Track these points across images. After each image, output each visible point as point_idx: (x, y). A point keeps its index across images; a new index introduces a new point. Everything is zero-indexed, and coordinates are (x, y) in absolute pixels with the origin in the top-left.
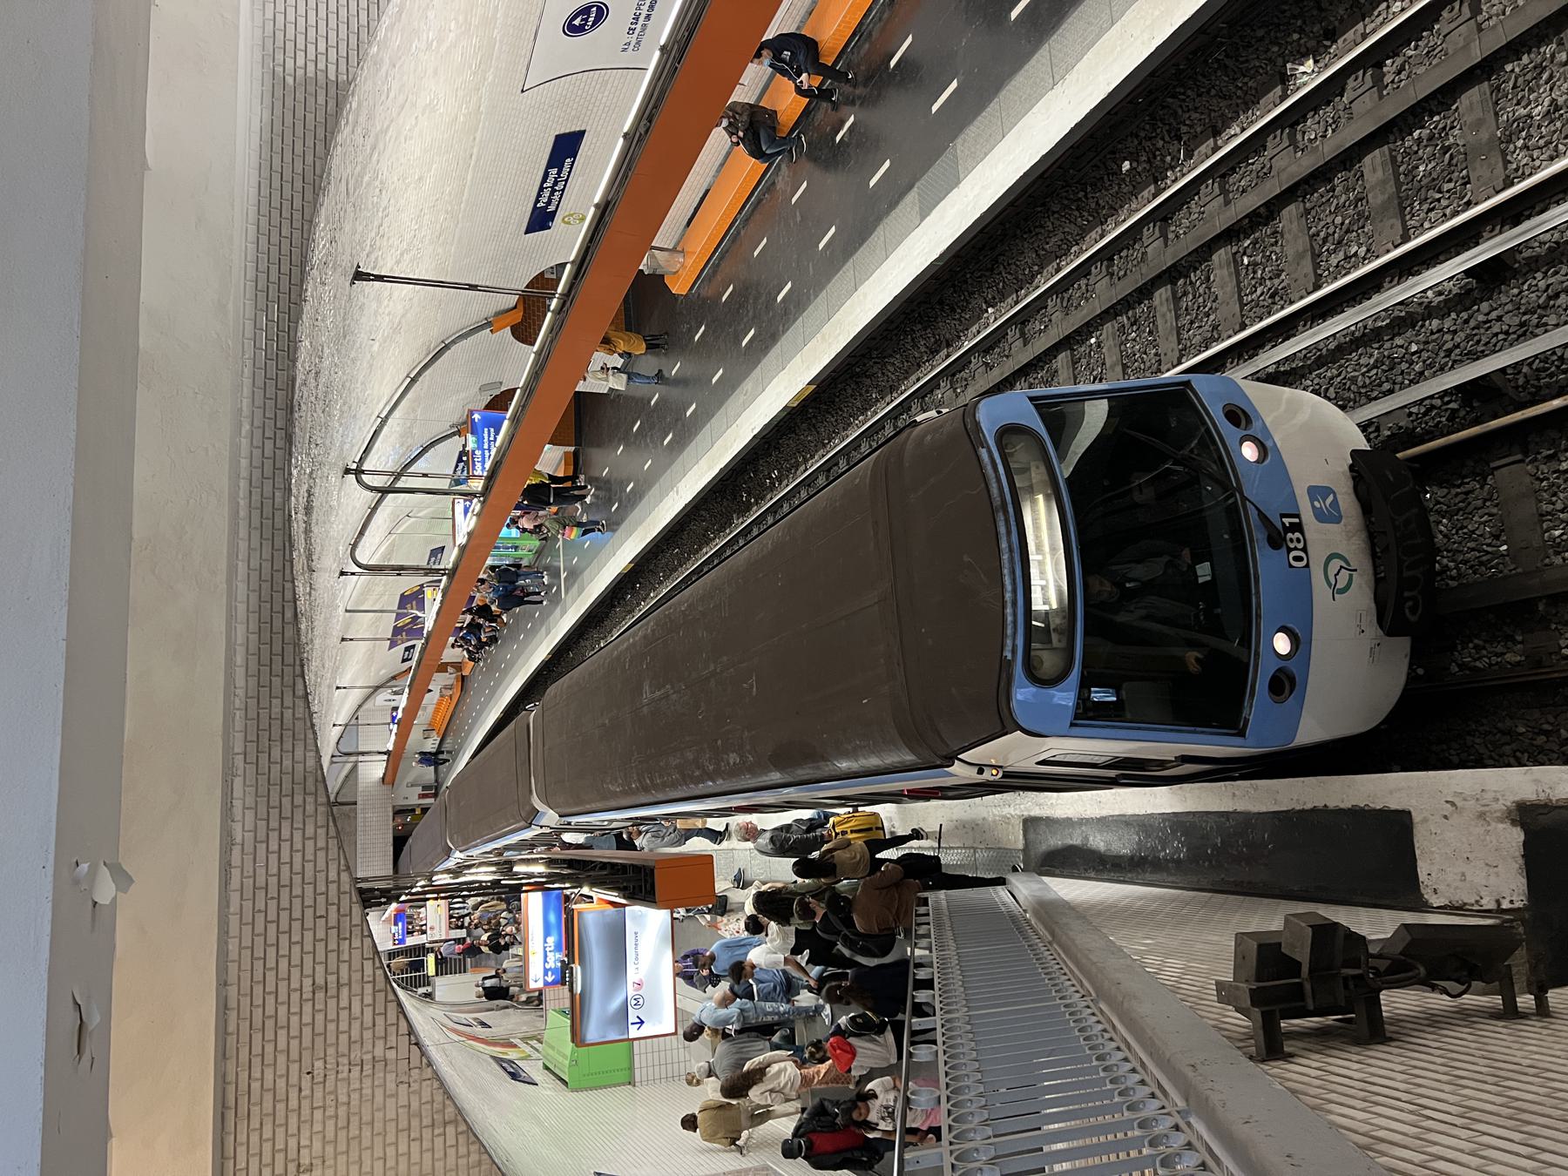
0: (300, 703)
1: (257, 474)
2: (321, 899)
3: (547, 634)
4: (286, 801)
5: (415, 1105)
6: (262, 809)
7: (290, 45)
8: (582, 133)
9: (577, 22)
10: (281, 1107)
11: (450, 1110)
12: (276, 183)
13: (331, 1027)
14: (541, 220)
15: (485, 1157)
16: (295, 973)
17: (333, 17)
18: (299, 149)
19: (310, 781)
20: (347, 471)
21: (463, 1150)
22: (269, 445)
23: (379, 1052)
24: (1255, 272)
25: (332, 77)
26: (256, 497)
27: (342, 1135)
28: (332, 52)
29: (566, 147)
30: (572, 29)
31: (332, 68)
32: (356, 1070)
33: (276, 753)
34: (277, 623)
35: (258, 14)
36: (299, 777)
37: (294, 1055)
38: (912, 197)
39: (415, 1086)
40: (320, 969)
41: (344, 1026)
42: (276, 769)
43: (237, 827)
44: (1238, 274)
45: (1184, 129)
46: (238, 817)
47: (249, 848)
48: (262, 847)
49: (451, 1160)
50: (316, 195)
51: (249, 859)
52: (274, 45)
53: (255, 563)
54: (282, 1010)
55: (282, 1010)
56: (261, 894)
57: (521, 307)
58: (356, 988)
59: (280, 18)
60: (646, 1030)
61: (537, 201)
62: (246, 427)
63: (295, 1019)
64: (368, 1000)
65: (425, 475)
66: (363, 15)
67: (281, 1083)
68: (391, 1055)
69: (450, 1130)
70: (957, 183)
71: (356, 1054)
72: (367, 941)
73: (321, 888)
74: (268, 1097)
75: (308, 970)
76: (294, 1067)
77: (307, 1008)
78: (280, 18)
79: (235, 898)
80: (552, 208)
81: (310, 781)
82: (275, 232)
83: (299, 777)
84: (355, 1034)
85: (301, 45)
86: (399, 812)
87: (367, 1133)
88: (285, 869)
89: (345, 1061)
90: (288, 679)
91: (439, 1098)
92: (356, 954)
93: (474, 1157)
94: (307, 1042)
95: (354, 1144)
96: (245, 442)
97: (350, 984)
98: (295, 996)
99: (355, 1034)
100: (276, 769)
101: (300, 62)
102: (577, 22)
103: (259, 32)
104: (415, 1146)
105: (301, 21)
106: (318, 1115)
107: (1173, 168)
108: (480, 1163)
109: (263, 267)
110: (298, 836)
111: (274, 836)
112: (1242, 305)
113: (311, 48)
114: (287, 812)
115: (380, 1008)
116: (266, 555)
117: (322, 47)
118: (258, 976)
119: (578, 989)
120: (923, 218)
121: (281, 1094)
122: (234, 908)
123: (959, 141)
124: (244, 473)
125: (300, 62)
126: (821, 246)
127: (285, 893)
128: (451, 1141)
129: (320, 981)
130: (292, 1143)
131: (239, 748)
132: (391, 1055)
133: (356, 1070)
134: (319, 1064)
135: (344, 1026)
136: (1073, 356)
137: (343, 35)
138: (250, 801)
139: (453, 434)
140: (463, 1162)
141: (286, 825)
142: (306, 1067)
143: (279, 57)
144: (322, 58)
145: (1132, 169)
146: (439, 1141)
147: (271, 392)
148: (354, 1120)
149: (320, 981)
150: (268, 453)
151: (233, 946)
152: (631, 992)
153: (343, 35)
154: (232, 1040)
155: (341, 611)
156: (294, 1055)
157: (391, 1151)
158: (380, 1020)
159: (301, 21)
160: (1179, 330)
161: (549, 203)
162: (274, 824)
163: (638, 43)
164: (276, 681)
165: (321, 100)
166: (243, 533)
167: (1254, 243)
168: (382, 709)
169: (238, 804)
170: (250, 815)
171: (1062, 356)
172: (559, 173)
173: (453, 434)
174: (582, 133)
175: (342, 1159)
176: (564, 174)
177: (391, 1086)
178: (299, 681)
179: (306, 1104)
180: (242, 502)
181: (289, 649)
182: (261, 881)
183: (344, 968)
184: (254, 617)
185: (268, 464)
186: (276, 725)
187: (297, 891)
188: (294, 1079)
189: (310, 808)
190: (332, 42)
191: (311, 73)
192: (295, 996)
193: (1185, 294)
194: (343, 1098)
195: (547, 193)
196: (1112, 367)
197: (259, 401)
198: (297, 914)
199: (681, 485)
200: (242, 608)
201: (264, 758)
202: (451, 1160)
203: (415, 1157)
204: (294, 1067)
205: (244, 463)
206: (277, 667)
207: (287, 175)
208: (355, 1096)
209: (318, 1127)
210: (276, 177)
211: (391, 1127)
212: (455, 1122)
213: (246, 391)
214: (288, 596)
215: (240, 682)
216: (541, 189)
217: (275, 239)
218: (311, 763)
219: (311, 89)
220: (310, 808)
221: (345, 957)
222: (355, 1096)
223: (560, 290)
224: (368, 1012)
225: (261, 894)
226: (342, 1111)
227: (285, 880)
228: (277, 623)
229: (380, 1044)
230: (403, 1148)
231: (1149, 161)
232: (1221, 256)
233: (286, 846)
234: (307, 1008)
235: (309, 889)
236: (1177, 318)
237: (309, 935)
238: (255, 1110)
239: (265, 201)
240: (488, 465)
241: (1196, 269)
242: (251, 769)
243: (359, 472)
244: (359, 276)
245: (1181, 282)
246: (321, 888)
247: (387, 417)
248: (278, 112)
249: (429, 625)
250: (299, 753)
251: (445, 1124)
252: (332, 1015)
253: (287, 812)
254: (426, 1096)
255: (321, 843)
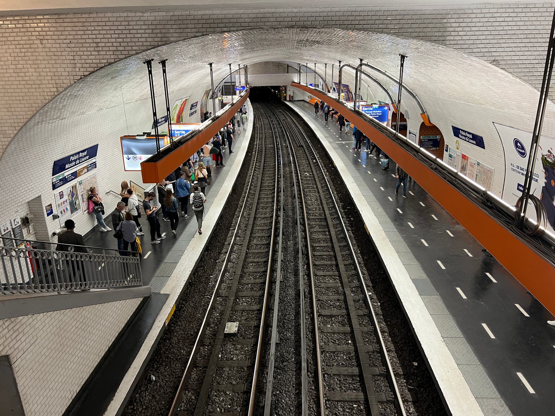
0: (192, 35)
1: (278, 15)
2: (126, 44)
3: (325, 137)
4: (158, 31)
5: (62, 78)
6: (155, 23)
7: (461, 20)
8: (484, 148)
9: (518, 144)
10: (59, 33)
11: (61, 90)
12: (398, 17)
13: (85, 49)
14: (457, 132)
15: (47, 101)
16: (102, 36)
17: (476, 37)
18: (413, 26)
19: (166, 39)
20: (361, 60)
21: (49, 94)
22: (290, 19)
23: (78, 65)
24: (349, 409)
25: (448, 38)
26: (268, 15)
27: (52, 54)
28: (460, 38)
29: (479, 141)
30: (516, 142)
31: (452, 38)
32: (71, 58)
33: (175, 26)
34: (222, 25)
35: (475, 7)
36: (167, 35)
37: (76, 37)
38: (424, 276)
39: (68, 77)
40: (103, 45)
41: (86, 53)
42: (169, 27)
43: (149, 14)
44: (351, 402)
45: (422, 390)
46: (152, 14)
47: (142, 18)
48: (142, 23)
49: (46, 90)
50: (394, 34)
51: (138, 19)
52: (461, 14)
53: (243, 16)
54: (90, 32)
55: (90, 32)
56: (126, 23)
57: (430, 125)
58: (98, 57)
59: (474, 16)
60: (126, 160)
61: (462, 130)
62: (295, 10)
63: (87, 36)
64: (94, 61)
65: (360, 89)
66: (478, 50)
67: (67, 33)
68: (77, 69)
69: (55, 89)
70: (420, 295)
71: (77, 57)
72: (113, 61)
73: (130, 44)
74: (62, 29)
75: (103, 40)
76: (72, 37)
77: (91, 41)
78: (474, 16)
79: (125, 14)
80: (460, 136)
81: (166, 39)
82: (377, 18)
83: (167, 35)
84: (83, 57)
85: (461, 25)
86: (285, 87)
87: (53, 62)
88: (135, 31)
89: (75, 54)
90: (201, 30)
91: (65, 86)
92: (108, 57)
93: (47, 98)
94: (80, 41)
95: (49, 58)
96: (289, 10)
97: (99, 55)
98: (94, 36)
99: (83, 57)
100: (169, 27)
101: (453, 25)
102: (518, 144)
103: (467, 7)
104: (49, 78)
105: (473, 24)
106: (58, 45)
107: (407, 383)
108: (45, 99)
109: (361, 14)
110: (147, 35)
111: (146, 27)
112: (338, 401)
113: (461, 29)
114: (155, 31)
115: (92, 65)
116: (247, 20)
117: (461, 33)
118: (100, 24)
119: (137, 138)
120: (412, 280)
121: (64, 33)
122: (122, 14)
123: (439, 297)
124: (277, 10)
125: (453, 25)
126: (423, 241)
127: (127, 32)
128: (52, 90)
129: (100, 45)
130: (49, 37)
131: (176, 13)
132: (77, 69)
133: (71, 58)
134: (73, 45)
135: (86, 53)
136: (347, 333)
137: (467, 42)
138: (158, 18)
139: (392, 101)
140: (46, 94)
141: (150, 31)
142: (73, 41)
143: (456, 16)
144: (456, 34)
145: (413, 365)
146: (51, 86)
147: (311, 19)
148: (57, 58)
149: (100, 45)
150: (286, 19)
151: (109, 15)
152: (138, 156)
153: (467, 42)
154: (79, 16)
155: (333, 63)
156: (76, 37)
157: (48, 70)
158: (88, 65)
159: (473, 24)
160: (339, 375)
161: (462, 135)
162: (150, 27)
163: (514, 170)
164: (200, 26)
165: (437, 34)
166: (254, 11)
167: (361, 410)
168: (318, 81)
169: (156, 14)
170: (153, 18)
171: (349, 329)
172: (470, 139)
173: (392, 101)
174: (484, 148)
175: (45, 54)
176: (471, 141)
177: (68, 70)
178: (201, 34)
179: (61, 41)
180: (266, 10)
181: (212, 30)
182: (131, 23)
183: (104, 53)
184: (223, 16)
185: (282, 19)
186: (185, 26)
187: (128, 36)
188: (68, 37)
189: (156, 39)
190: (464, 38)
191: (448, 29)
192: (94, 36)
193: (353, 380)
194: (63, 54)
195: (464, 134)
196: (336, 348)
197: (306, 15)
198: (120, 36)
199: (355, 184)
200: (226, 12)
201: (173, 22)
202: (46, 90)
203: (46, 78)
204: (72, 37)
205: (281, 10)
206: (206, 26)
207: (401, 22)
208: (64, 58)
209: (54, 45)
210: (401, 17)
211: (55, 70)
212: (57, 91)
213: (310, 10)
214: (232, 29)
215: (199, 13)
216: (465, 132)
217: (374, 18)
218: (172, 39)
219: (442, 30)
220: (156, 39)
221: (108, 53)
222: (64, 58)
223: (399, 135)
224: (91, 61)
225: (126, 23)
226: (59, 53)
227: (132, 31)
228: (222, 25)
229: (80, 65)
230: (49, 74)
231: (413, 373)
232: (361, 395)
233: (143, 31)
234: (91, 41)
235: (129, 40)
236: (344, 375)
237: (114, 40)
238: (58, 25)
239: (390, 13)
240: (363, 112)
241: (360, 385)
242: (169, 18)
243: (361, 65)
244: (403, 57)
245: (358, 379)
246: (130, 44)
247: (386, 75)
248: (430, 17)
249: (329, 95)
250: (176, 35)
251: (57, 88)
252: (89, 49)
253: (155, 31)
254: (65, 81)
255: (145, 44)
